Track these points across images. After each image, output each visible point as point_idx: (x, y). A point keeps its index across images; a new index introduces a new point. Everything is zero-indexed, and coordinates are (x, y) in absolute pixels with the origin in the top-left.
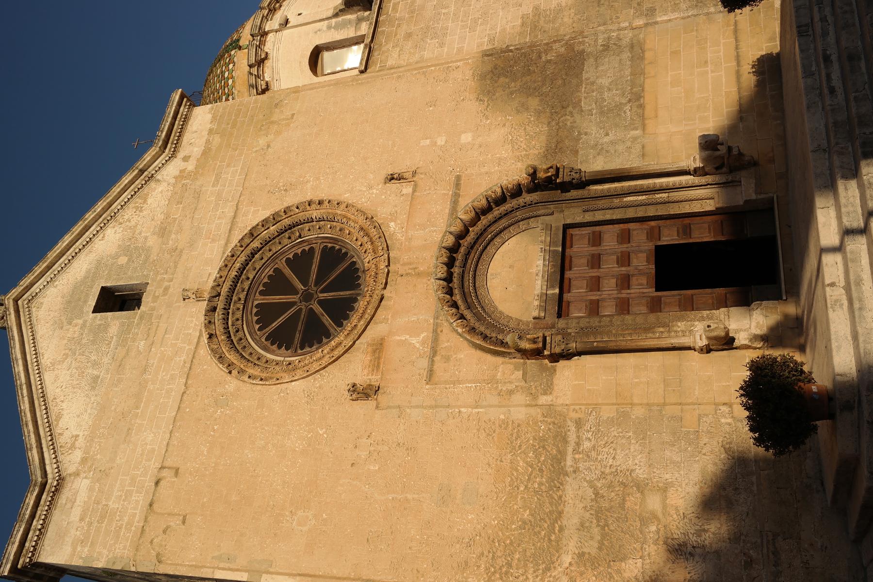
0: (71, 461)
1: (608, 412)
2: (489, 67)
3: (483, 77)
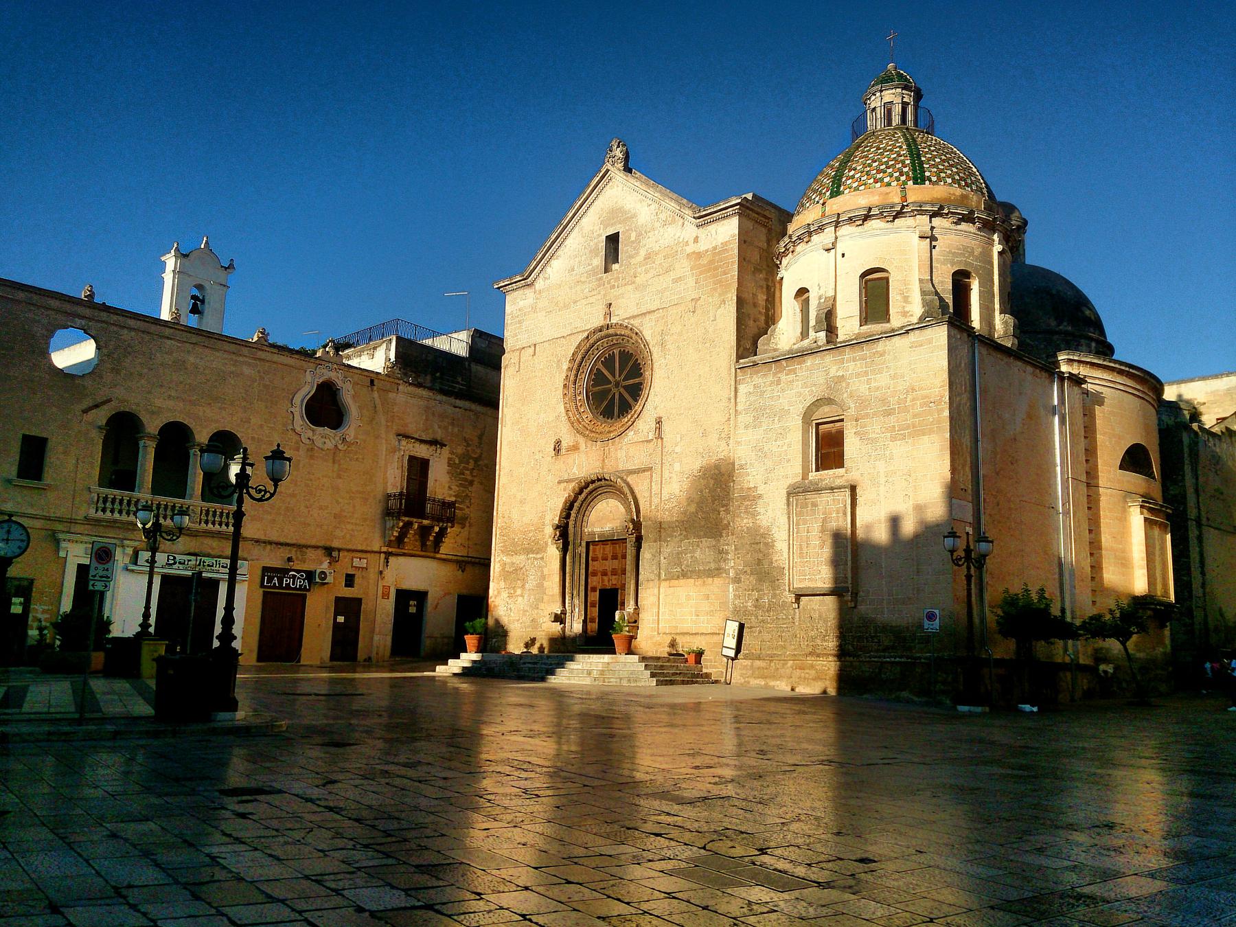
0: (540, 284)
1: (546, 571)
2: (723, 470)
3: (717, 467)
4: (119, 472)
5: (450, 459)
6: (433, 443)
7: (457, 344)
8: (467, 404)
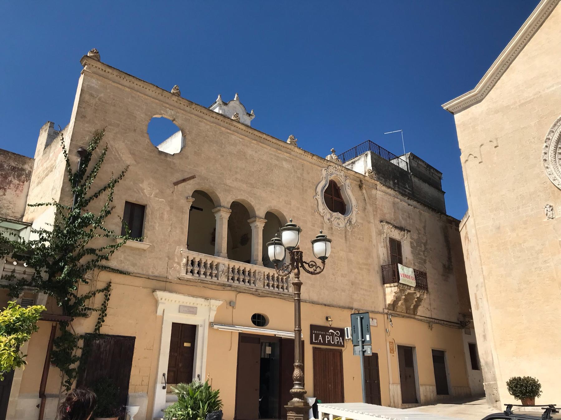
4: (201, 238)
5: (411, 243)
6: (401, 229)
7: (402, 162)
8: (415, 203)
